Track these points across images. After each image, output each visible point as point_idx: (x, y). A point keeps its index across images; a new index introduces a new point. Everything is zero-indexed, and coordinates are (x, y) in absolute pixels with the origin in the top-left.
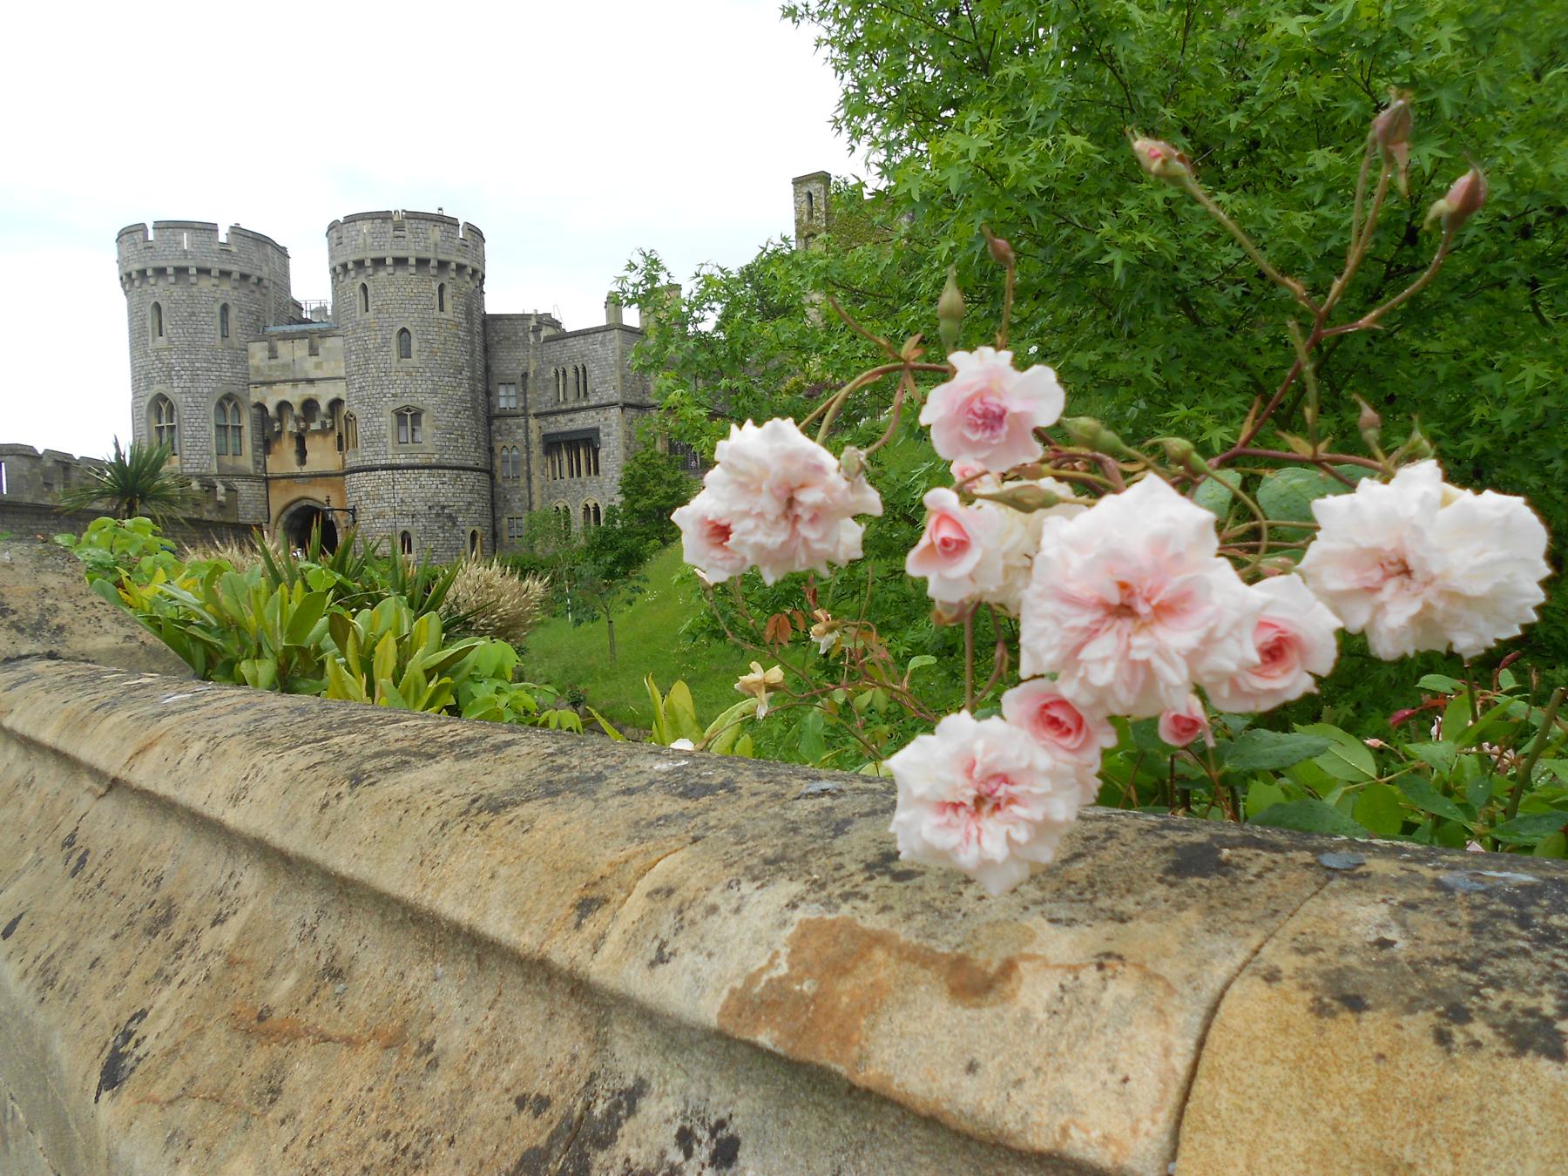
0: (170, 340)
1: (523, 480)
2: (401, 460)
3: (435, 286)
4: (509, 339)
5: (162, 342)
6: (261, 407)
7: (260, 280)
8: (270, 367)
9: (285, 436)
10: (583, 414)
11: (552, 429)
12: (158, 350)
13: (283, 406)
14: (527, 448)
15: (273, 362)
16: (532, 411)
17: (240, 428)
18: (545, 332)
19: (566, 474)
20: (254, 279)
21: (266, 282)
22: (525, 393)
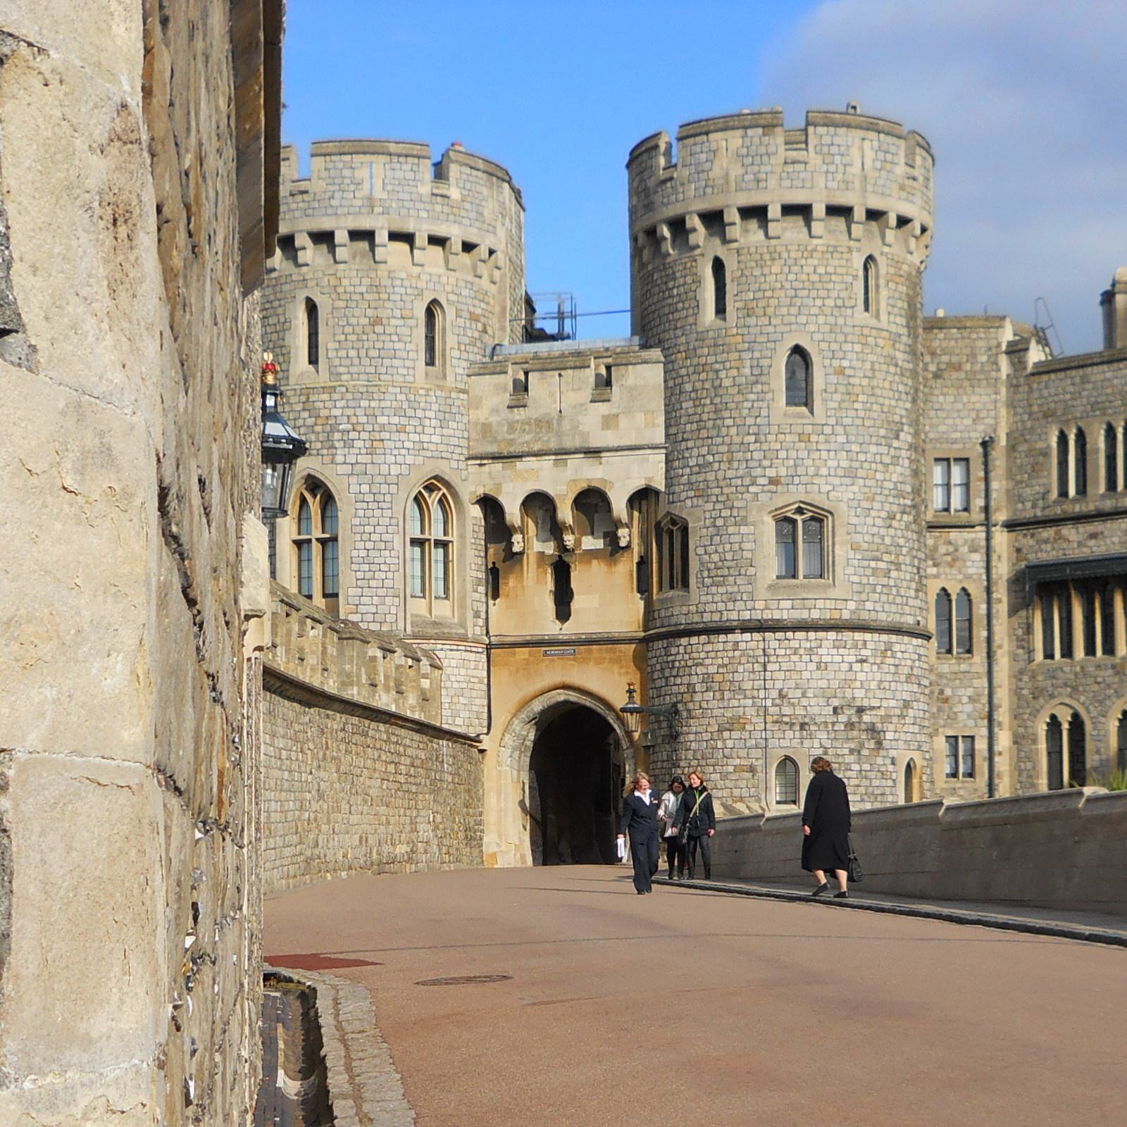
1: (979, 657)
2: (784, 611)
3: (858, 262)
4: (958, 367)
6: (490, 505)
7: (491, 252)
8: (511, 426)
9: (530, 563)
12: (308, 392)
13: (539, 503)
14: (989, 591)
15: (519, 414)
16: (1001, 516)
17: (444, 545)
18: (1035, 355)
21: (500, 257)
22: (987, 480)
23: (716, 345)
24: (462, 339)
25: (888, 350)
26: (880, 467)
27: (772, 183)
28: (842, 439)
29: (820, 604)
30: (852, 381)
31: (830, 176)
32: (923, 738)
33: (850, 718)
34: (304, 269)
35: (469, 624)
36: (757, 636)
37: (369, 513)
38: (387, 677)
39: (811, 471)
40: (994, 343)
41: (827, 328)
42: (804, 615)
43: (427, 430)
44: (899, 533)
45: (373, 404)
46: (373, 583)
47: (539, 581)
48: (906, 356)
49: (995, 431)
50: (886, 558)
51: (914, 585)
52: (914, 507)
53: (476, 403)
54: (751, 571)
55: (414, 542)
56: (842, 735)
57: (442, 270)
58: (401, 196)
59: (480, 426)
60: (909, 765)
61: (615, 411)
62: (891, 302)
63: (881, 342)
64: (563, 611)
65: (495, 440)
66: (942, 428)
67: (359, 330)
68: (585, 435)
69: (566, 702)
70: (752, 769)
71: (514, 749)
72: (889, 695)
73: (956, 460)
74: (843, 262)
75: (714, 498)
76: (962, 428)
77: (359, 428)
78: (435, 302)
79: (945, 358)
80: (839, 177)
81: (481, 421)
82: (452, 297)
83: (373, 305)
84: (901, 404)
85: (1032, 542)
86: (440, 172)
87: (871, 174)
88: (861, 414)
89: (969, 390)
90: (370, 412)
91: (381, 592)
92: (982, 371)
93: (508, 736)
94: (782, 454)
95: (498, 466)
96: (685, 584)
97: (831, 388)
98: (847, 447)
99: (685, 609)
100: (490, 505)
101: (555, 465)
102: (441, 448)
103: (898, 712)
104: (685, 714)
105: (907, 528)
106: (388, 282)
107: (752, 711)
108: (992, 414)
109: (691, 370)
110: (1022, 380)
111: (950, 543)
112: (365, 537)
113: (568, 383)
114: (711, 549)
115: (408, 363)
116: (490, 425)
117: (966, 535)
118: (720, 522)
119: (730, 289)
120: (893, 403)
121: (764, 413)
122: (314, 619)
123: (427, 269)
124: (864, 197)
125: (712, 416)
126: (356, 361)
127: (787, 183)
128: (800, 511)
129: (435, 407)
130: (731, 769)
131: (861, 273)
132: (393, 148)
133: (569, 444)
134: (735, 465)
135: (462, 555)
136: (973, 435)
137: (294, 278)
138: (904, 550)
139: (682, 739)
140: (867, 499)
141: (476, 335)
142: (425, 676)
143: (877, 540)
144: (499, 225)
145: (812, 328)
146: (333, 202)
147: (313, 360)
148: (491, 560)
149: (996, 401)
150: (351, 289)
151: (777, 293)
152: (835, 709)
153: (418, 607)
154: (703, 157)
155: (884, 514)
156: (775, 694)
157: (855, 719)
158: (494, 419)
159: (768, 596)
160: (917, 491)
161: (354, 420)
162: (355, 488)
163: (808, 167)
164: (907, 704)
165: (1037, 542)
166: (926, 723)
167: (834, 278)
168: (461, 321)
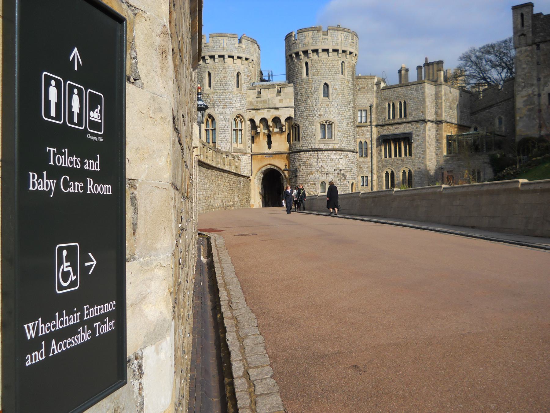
0: (215, 90)
2: (322, 146)
3: (340, 63)
4: (364, 88)
5: (212, 90)
6: (252, 121)
8: (257, 102)
9: (262, 135)
10: (403, 125)
11: (385, 133)
12: (208, 94)
15: (259, 99)
16: (374, 124)
18: (382, 85)
19: (393, 156)
20: (250, 60)
21: (254, 61)
22: (371, 115)
23: (306, 83)
24: (245, 81)
25: (347, 84)
26: (345, 112)
27: (320, 44)
28: (336, 105)
29: (331, 145)
30: (339, 91)
31: (333, 42)
32: (355, 177)
33: (338, 172)
34: (208, 64)
35: (247, 150)
36: (316, 152)
37: (223, 123)
38: (227, 162)
39: (329, 113)
40: (373, 82)
41: (333, 79)
42: (327, 147)
43: (237, 103)
44: (350, 128)
45: (224, 97)
46: (224, 140)
47: (264, 139)
48: (352, 85)
49: (373, 103)
50: (347, 133)
51: (353, 140)
52: (353, 121)
53: (249, 97)
54: (315, 137)
55: (234, 130)
56: (336, 176)
57: (241, 65)
58: (231, 47)
59: (249, 102)
60: (352, 183)
61: (282, 99)
62: (348, 72)
63: (346, 82)
64: (270, 146)
65: (253, 105)
66: (360, 103)
67: (221, 79)
68: (275, 104)
69: (270, 168)
70: (315, 184)
71: (258, 179)
72: (347, 166)
73: (363, 110)
74: (337, 63)
75: (306, 119)
76: (364, 102)
77: (221, 102)
78: (239, 72)
79: (361, 86)
80: (336, 42)
81: (250, 101)
82: (243, 71)
83: (224, 73)
84: (350, 97)
85: (382, 130)
86: (240, 41)
87: (343, 42)
88: (341, 99)
89: (367, 93)
90: (223, 99)
91: (226, 142)
92: (370, 89)
93: (256, 176)
94: (322, 109)
95: (254, 112)
96: (299, 140)
97: (334, 93)
98: (337, 107)
99: (299, 146)
100: (252, 121)
101: (268, 111)
102: (240, 107)
103: (350, 170)
104: (299, 171)
105: (352, 126)
106: (228, 68)
107: (315, 170)
108: (372, 99)
109: (300, 89)
110: (379, 91)
111: (362, 130)
112: (222, 129)
113: (271, 92)
114: (305, 131)
115: (232, 87)
116: (252, 102)
117: (366, 128)
118: (307, 125)
119: (310, 69)
120: (349, 96)
121: (318, 99)
122: (210, 148)
123: (237, 64)
124: (342, 47)
125: (305, 100)
126: (220, 87)
127: (323, 44)
128: (326, 122)
129: (239, 98)
130: (310, 184)
131: (341, 65)
132: (229, 35)
133: (271, 106)
134: (311, 111)
135: (245, 133)
136: (367, 104)
137: (205, 66)
138: (351, 132)
139: (298, 177)
140: (342, 120)
141: (249, 80)
142: (237, 162)
143: (345, 129)
144: (254, 54)
145: (329, 79)
146: (215, 48)
147: (210, 86)
148: (252, 134)
149: (373, 96)
150: (219, 69)
151: (321, 70)
152: (335, 170)
153: (235, 145)
154: (303, 38)
155: (346, 123)
156: (320, 166)
157: (339, 172)
158: (253, 100)
159: (319, 143)
160: (354, 118)
161: (219, 101)
162: (220, 117)
163: (328, 40)
164: (352, 169)
165: (383, 130)
166: (356, 173)
167: (334, 67)
168: (245, 77)
